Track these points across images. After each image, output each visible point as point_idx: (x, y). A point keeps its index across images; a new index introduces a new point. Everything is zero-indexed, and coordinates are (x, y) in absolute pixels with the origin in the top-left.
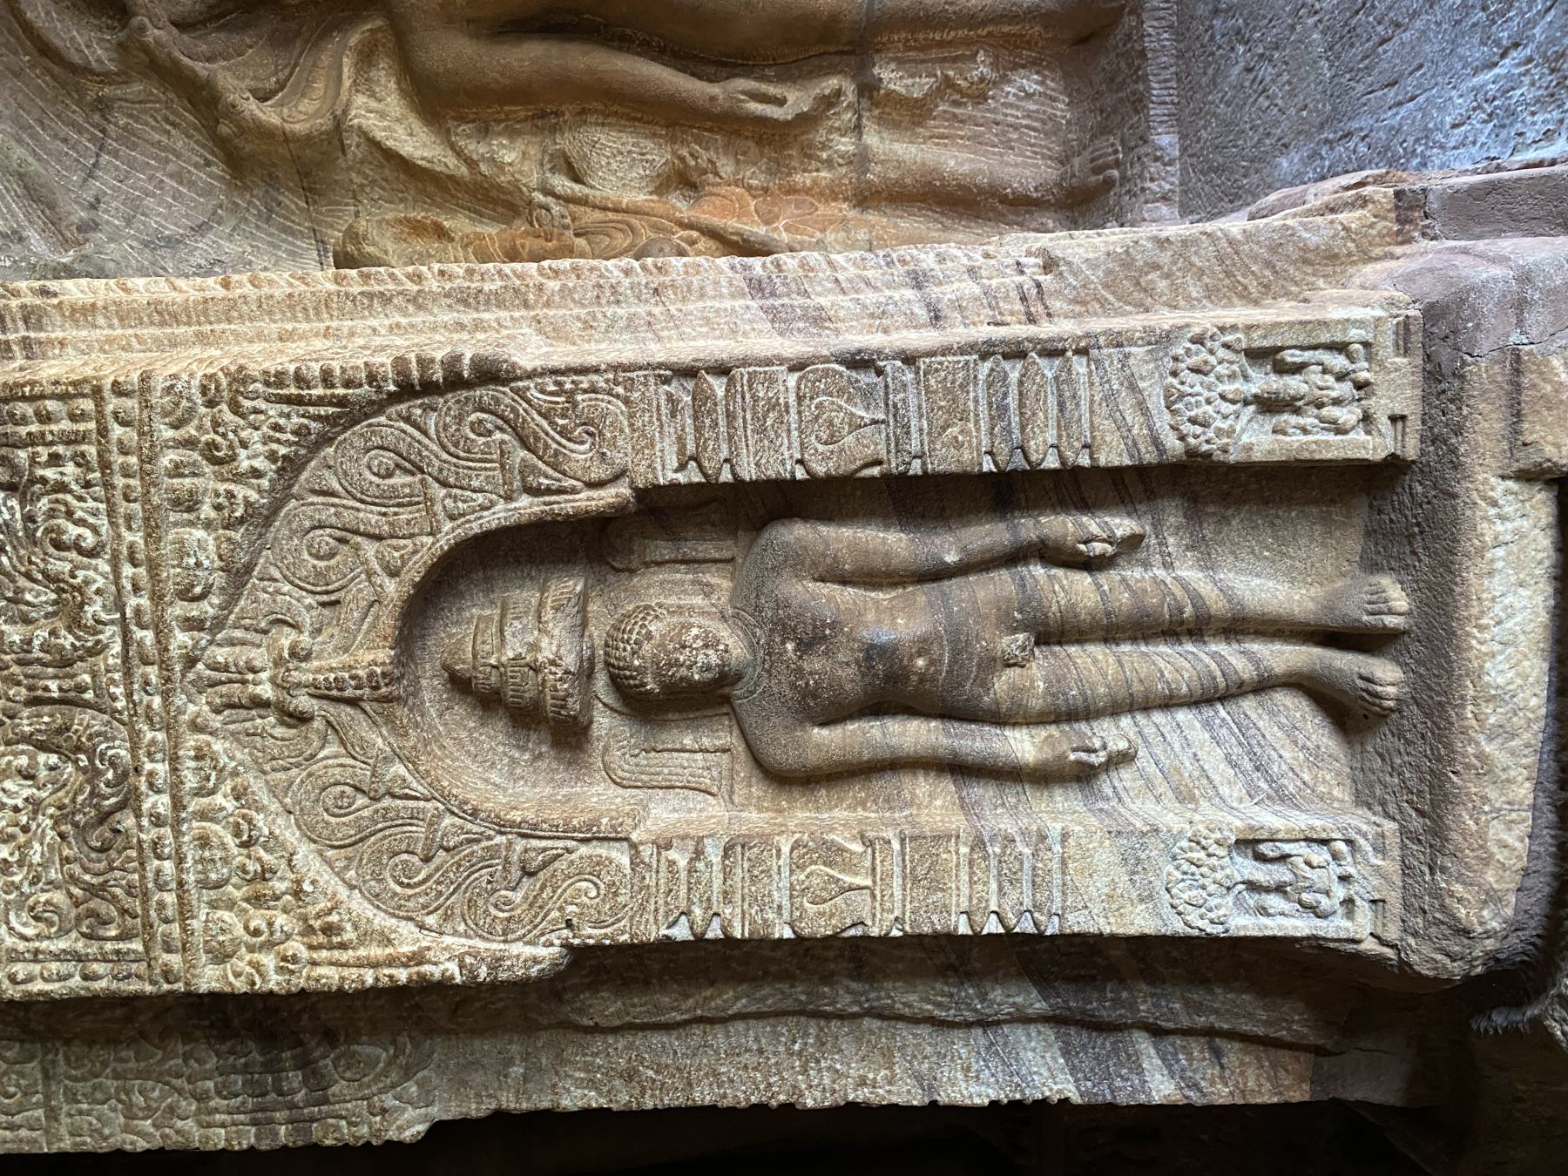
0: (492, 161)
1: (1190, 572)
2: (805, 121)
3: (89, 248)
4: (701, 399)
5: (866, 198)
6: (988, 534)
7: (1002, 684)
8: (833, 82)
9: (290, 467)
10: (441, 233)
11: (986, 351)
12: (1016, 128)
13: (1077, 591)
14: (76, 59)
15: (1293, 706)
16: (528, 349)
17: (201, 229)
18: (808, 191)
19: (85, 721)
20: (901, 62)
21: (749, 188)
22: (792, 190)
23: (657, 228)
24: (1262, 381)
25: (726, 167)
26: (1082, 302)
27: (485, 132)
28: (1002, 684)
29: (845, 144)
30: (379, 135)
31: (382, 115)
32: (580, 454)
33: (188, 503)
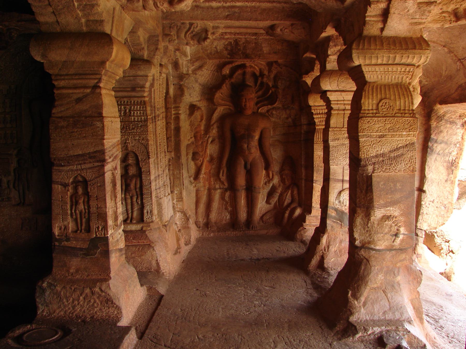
0: (213, 129)
1: (136, 209)
2: (220, 179)
3: (192, 75)
4: (148, 172)
5: (209, 190)
6: (139, 193)
7: (128, 194)
8: (226, 184)
9: (142, 144)
10: (202, 120)
11: (151, 192)
12: (221, 215)
13: (135, 200)
14: (223, 70)
15: (126, 217)
16: (151, 160)
17: (200, 84)
18: (210, 180)
19: (125, 129)
20: (230, 195)
21: (210, 171)
22: (210, 178)
23: (202, 156)
24: (149, 211)
25: (214, 166)
26: (157, 201)
27: (218, 127)
28: (128, 194)
29: (217, 186)
30: (217, 111)
31: (220, 111)
32: (144, 164)
33: (140, 137)
